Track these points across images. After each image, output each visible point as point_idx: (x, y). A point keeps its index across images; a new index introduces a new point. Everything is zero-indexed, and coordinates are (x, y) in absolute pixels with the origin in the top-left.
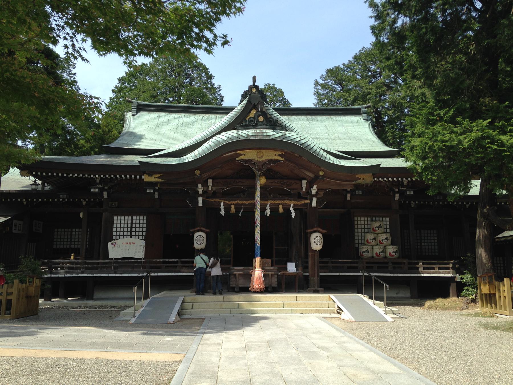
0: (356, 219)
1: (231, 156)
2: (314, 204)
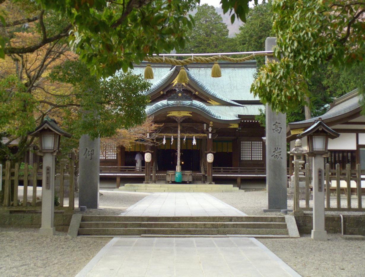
0: (242, 142)
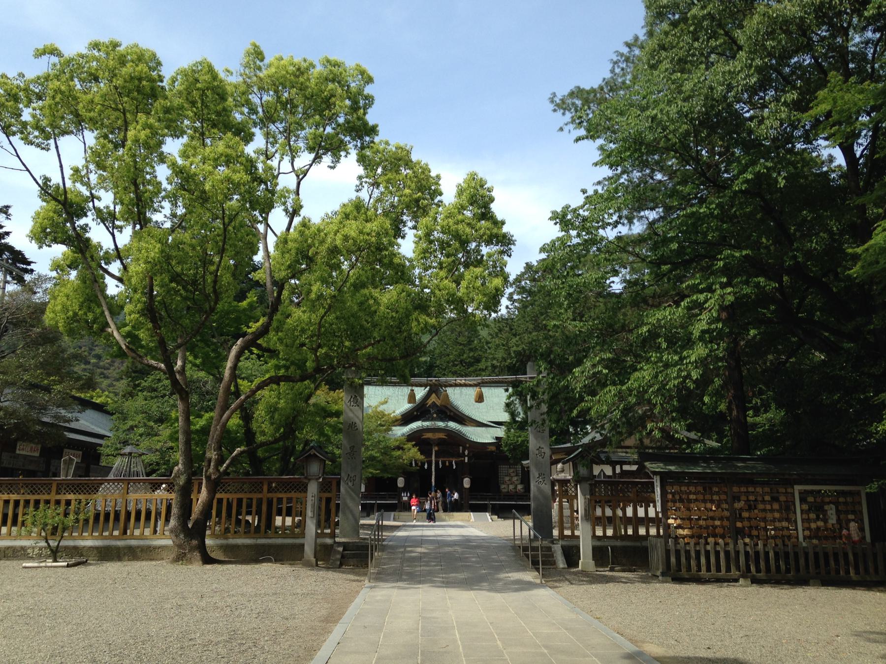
2: (466, 461)
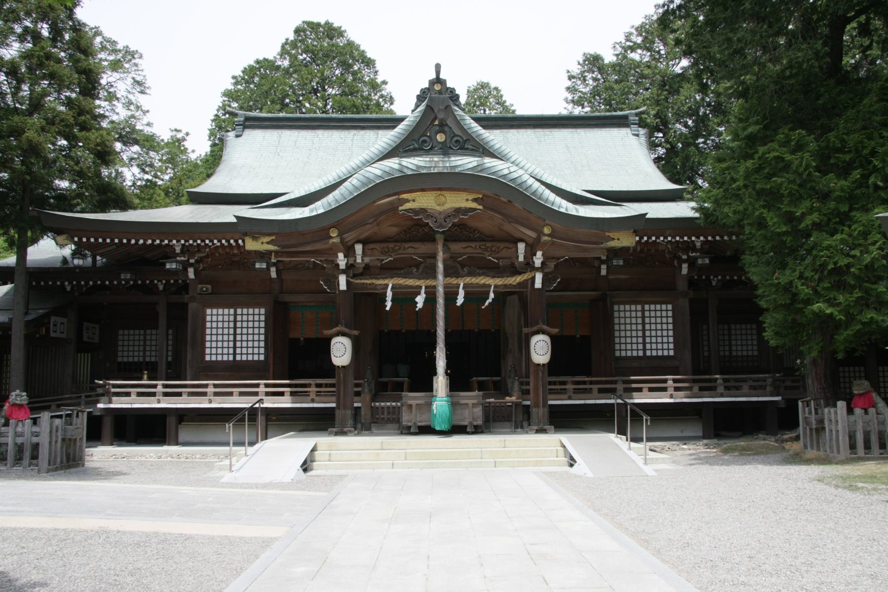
0: (616, 307)
1: (391, 203)
2: (538, 284)
